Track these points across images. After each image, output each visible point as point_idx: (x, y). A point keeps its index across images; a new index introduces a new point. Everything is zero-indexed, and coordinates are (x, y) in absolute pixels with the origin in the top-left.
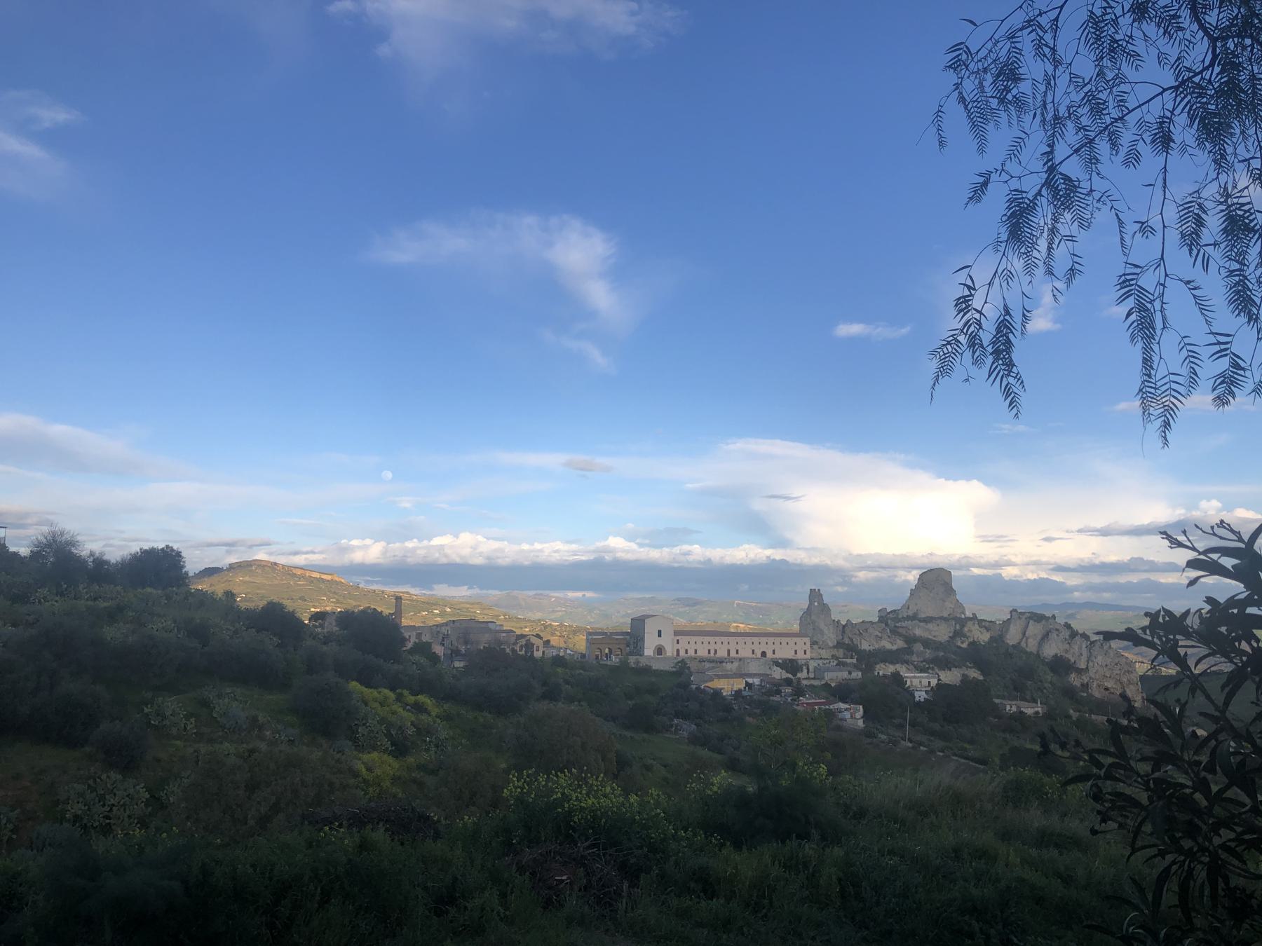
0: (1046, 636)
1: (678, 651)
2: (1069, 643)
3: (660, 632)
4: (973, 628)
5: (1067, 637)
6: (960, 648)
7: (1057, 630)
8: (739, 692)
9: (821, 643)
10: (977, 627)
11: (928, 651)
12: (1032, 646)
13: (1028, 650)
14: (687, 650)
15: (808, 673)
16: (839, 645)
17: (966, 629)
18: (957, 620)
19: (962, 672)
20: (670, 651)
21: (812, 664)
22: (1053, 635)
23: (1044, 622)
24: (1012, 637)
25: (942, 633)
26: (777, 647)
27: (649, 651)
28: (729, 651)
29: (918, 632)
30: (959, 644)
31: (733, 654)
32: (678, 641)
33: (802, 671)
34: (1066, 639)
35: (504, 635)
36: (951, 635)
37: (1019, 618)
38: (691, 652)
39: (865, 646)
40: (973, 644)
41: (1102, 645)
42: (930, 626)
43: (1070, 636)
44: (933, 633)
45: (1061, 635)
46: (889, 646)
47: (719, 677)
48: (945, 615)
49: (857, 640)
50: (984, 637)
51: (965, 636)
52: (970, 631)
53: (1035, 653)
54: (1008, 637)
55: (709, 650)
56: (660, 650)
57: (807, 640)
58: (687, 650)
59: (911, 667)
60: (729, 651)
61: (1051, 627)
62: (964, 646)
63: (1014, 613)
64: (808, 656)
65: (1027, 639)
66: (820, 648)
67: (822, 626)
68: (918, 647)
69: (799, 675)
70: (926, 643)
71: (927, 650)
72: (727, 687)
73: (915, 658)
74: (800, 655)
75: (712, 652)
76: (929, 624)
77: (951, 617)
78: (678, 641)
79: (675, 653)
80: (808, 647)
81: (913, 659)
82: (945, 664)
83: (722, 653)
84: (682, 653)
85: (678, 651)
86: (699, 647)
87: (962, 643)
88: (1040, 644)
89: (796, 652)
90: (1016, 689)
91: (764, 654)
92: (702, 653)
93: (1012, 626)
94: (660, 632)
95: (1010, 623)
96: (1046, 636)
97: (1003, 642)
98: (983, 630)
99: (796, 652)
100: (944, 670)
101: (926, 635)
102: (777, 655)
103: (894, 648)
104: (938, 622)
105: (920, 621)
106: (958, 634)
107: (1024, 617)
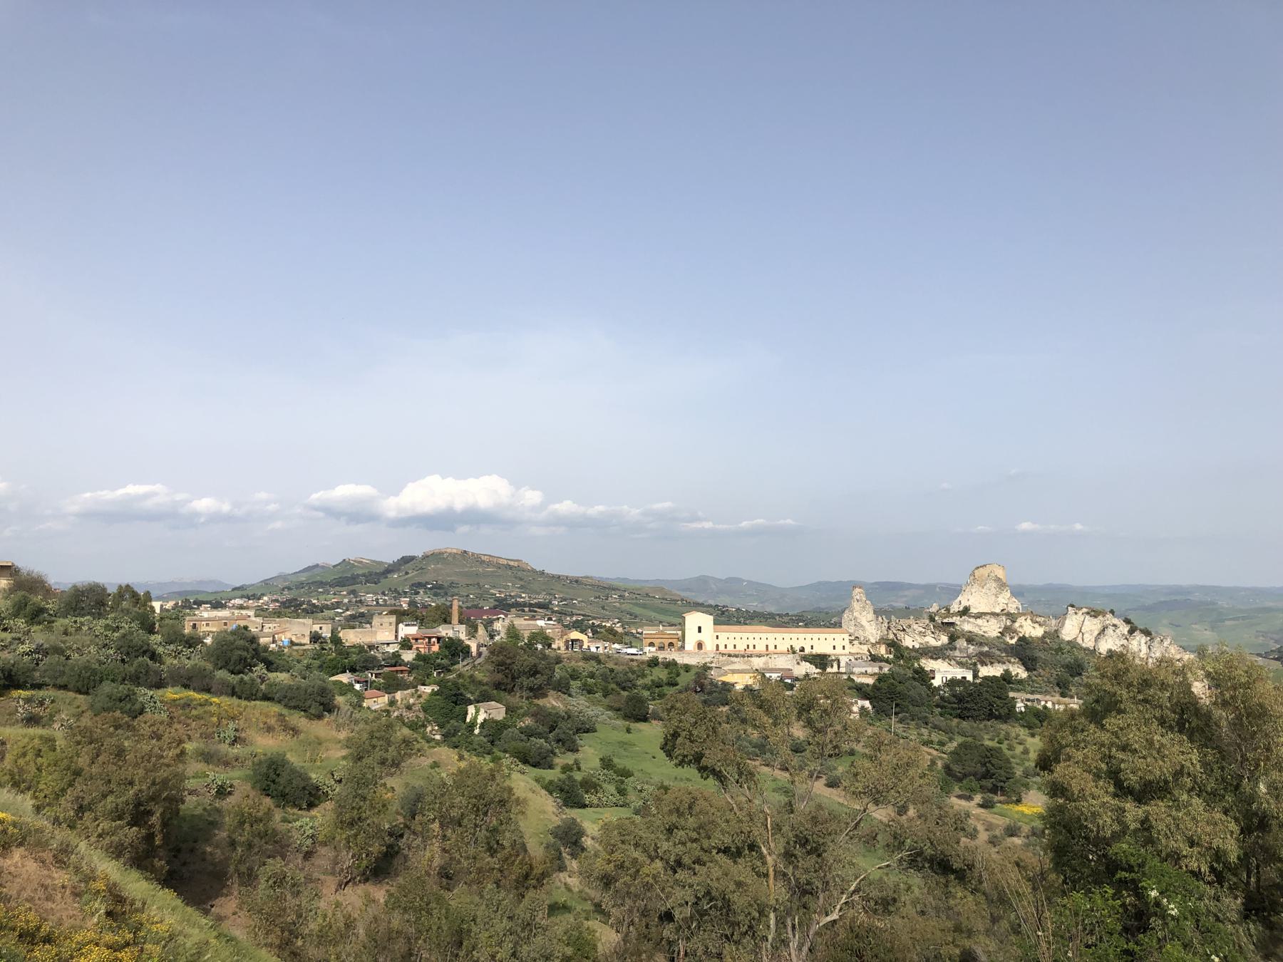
0: (1103, 631)
1: (717, 646)
2: (1126, 638)
3: (700, 628)
4: (1024, 623)
5: (1126, 633)
6: (1007, 644)
7: (1115, 625)
8: (748, 689)
9: (862, 639)
10: (1029, 621)
11: (972, 647)
12: (1088, 643)
13: (1084, 645)
14: (726, 646)
15: (839, 667)
16: (883, 640)
17: (1017, 625)
18: (1009, 615)
19: (1005, 668)
20: (709, 646)
21: (843, 661)
22: (1110, 631)
23: (1100, 617)
24: (1069, 631)
25: (991, 629)
26: (815, 643)
27: (690, 645)
28: (767, 646)
29: (967, 627)
30: (1008, 639)
31: (771, 648)
32: (717, 637)
33: (832, 666)
34: (1123, 635)
35: (550, 631)
36: (1001, 630)
37: (1076, 613)
38: (730, 648)
39: (908, 642)
40: (1023, 639)
41: (1162, 641)
42: (979, 621)
43: (1129, 632)
44: (984, 629)
45: (1117, 631)
46: (933, 643)
47: (734, 672)
48: (998, 610)
49: (901, 635)
50: (1038, 632)
51: (1015, 631)
52: (1021, 626)
53: (1092, 648)
54: (1063, 632)
55: (748, 646)
56: (700, 646)
57: (846, 637)
58: (726, 646)
59: (953, 662)
60: (767, 646)
61: (1108, 622)
62: (1013, 642)
63: (1070, 608)
64: (847, 651)
65: (1083, 634)
66: (861, 644)
67: (864, 622)
68: (962, 643)
69: (829, 670)
70: (970, 640)
71: (970, 646)
72: (741, 681)
73: (957, 653)
74: (839, 650)
75: (751, 647)
76: (978, 620)
77: (1005, 612)
78: (717, 637)
79: (715, 649)
80: (846, 643)
81: (956, 655)
82: (985, 659)
83: (761, 648)
84: (722, 648)
85: (717, 646)
86: (737, 642)
87: (1012, 638)
88: (1097, 639)
89: (834, 647)
90: (1058, 685)
91: (802, 650)
92: (741, 647)
93: (1067, 622)
94: (700, 628)
95: (1065, 619)
96: (1103, 631)
97: (1058, 637)
98: (1036, 625)
99: (834, 647)
100: (986, 665)
101: (976, 630)
102: (814, 652)
103: (939, 644)
104: (988, 617)
105: (970, 617)
106: (1007, 630)
107: (1081, 612)
